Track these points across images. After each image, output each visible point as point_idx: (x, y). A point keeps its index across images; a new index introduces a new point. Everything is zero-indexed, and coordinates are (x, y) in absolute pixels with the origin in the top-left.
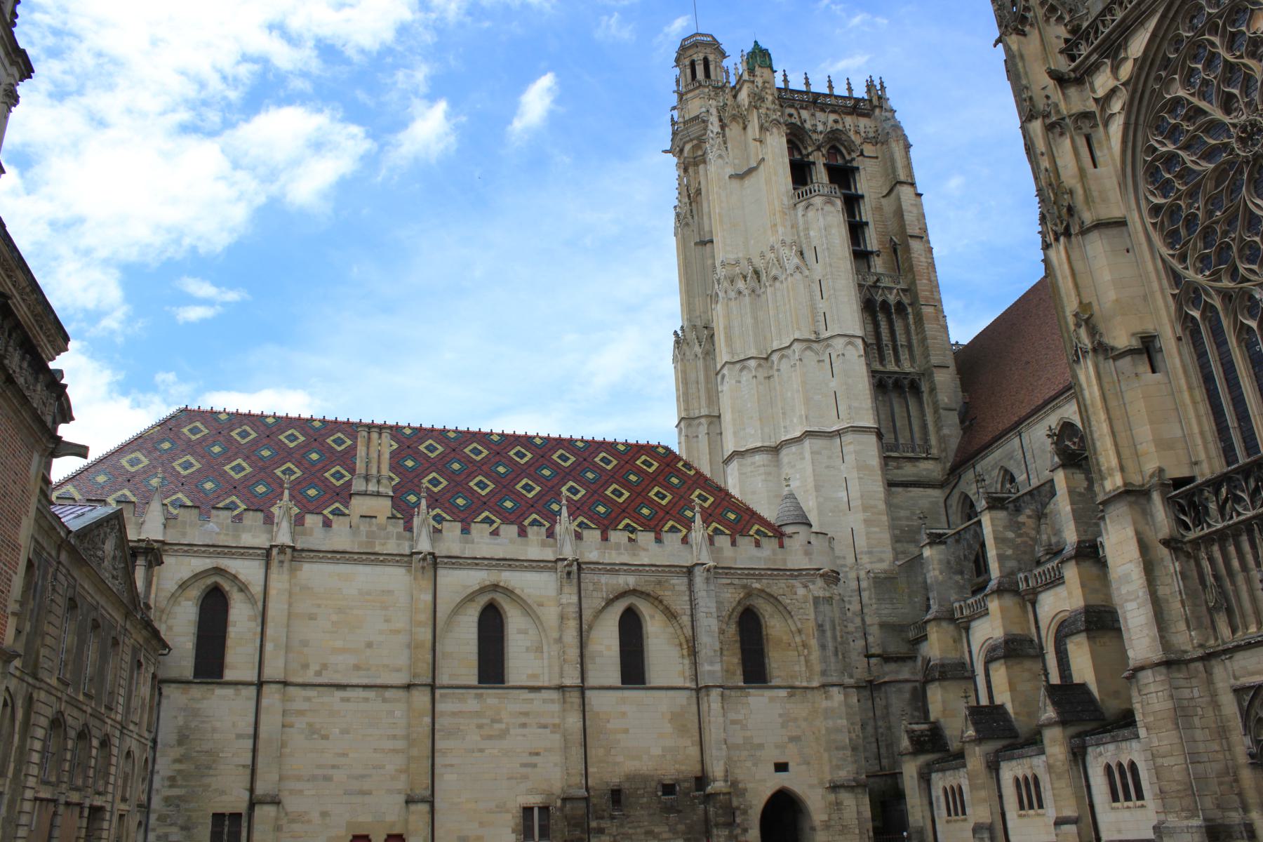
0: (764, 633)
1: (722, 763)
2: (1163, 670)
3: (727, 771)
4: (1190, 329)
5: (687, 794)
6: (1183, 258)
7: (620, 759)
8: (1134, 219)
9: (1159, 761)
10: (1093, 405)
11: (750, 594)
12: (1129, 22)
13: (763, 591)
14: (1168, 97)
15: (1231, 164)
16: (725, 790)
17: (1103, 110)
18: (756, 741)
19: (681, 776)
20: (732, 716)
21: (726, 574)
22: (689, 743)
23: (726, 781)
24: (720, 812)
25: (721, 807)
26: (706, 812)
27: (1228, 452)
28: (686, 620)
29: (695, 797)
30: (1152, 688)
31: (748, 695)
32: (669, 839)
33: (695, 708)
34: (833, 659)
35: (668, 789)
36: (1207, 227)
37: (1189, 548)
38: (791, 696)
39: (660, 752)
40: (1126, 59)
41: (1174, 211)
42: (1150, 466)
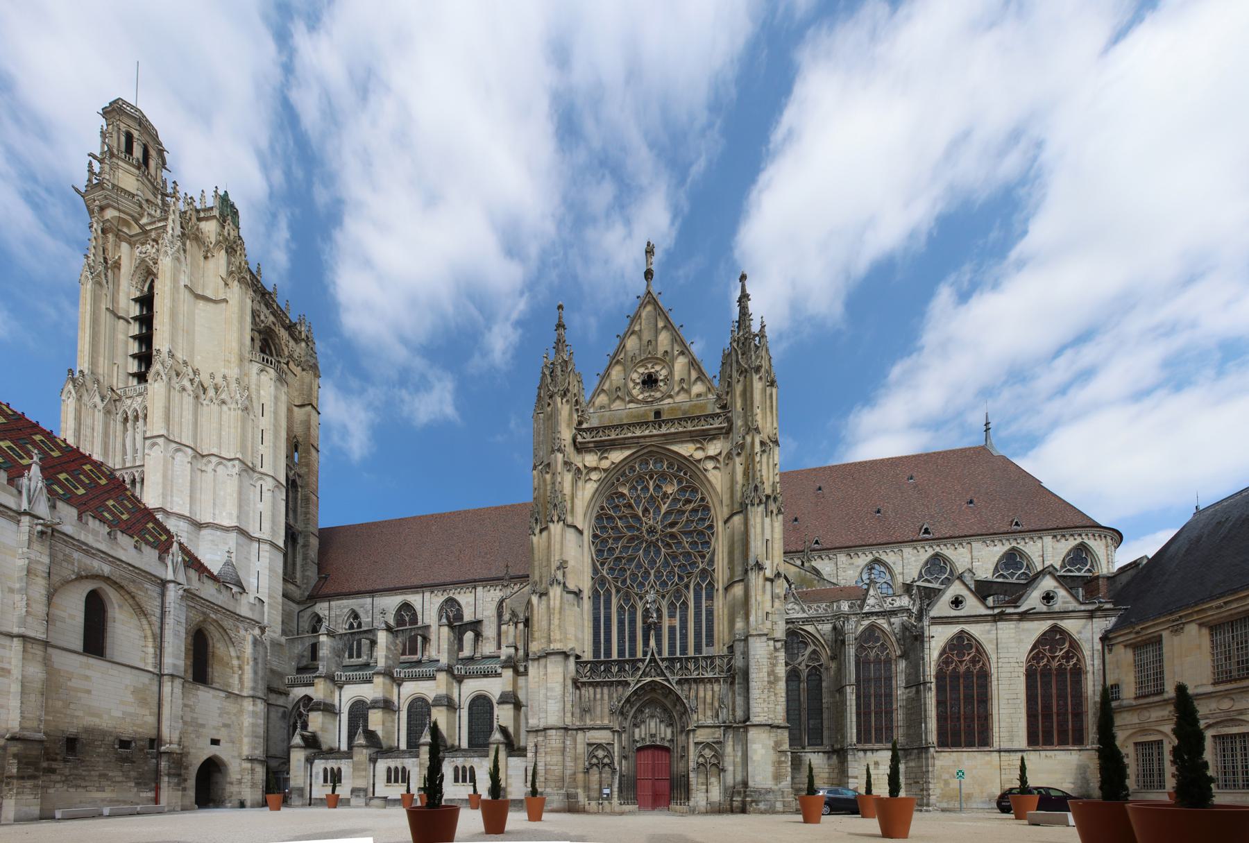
0: (210, 649)
1: (178, 732)
2: (563, 731)
3: (181, 738)
4: (595, 595)
5: (141, 750)
6: (602, 564)
7: (80, 713)
8: (586, 533)
9: (548, 767)
10: (554, 609)
11: (204, 621)
12: (617, 442)
13: (217, 621)
14: (620, 490)
15: (638, 538)
16: (178, 751)
17: (587, 473)
18: (200, 721)
19: (138, 736)
20: (186, 702)
21: (193, 598)
22: (147, 712)
23: (179, 745)
24: (172, 766)
25: (173, 763)
26: (158, 764)
27: (596, 652)
28: (155, 620)
29: (148, 753)
30: (554, 737)
31: (198, 689)
32: (122, 782)
33: (155, 688)
34: (260, 682)
35: (125, 744)
36: (618, 557)
37: (579, 685)
38: (227, 697)
39: (120, 715)
40: (607, 458)
41: (604, 541)
42: (570, 646)
